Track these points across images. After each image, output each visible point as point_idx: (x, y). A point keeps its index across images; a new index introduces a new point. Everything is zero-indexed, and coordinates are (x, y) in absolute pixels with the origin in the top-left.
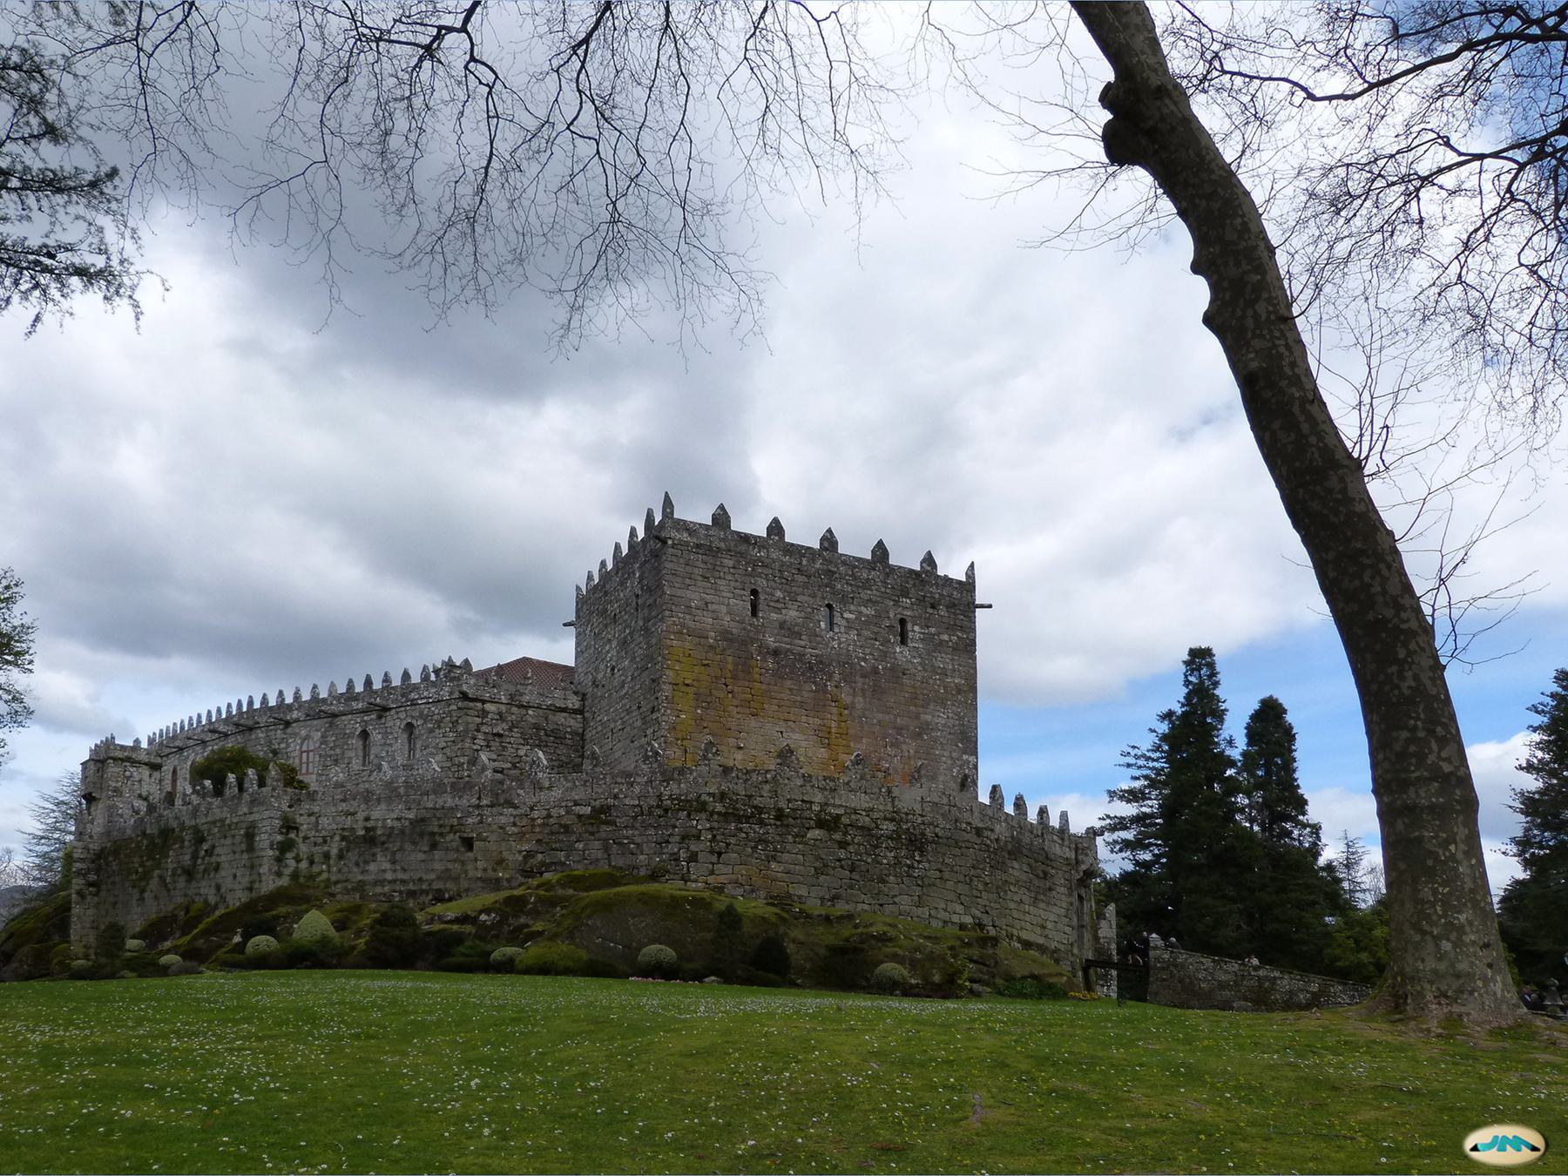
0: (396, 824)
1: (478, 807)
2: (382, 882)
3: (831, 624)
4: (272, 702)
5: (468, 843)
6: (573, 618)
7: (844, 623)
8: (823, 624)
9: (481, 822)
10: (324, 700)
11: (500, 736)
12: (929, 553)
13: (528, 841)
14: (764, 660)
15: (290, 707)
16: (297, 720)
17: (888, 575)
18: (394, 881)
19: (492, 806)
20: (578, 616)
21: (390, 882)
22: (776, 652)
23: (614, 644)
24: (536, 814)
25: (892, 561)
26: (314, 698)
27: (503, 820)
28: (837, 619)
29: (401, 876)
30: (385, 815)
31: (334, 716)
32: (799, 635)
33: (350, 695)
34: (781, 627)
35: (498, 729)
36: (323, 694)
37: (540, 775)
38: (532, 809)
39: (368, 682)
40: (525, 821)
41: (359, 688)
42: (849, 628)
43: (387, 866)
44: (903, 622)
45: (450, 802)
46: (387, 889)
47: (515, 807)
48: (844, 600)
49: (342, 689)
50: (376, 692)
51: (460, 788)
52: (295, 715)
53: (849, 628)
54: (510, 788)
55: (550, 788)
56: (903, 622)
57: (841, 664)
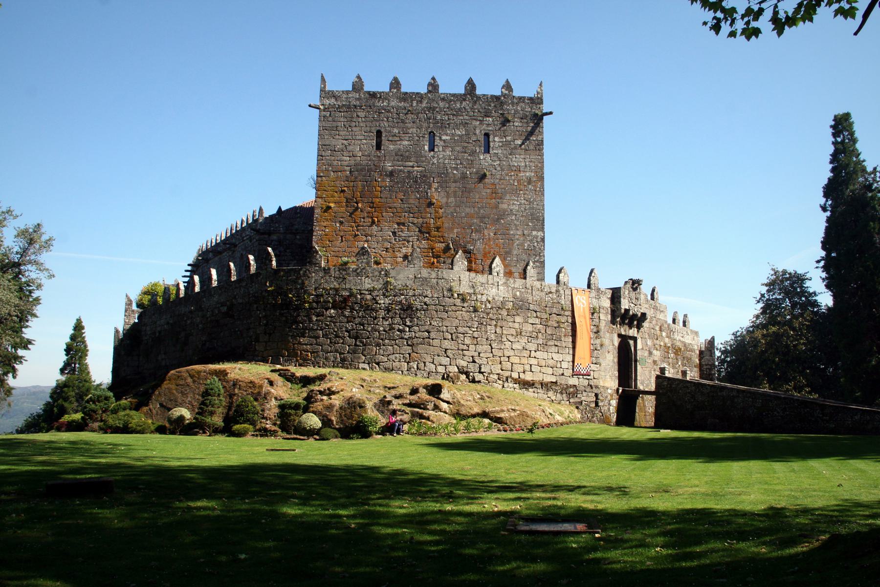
3: (432, 149)
7: (442, 143)
8: (426, 148)
12: (507, 81)
14: (383, 180)
17: (475, 102)
22: (391, 174)
25: (479, 92)
28: (437, 141)
32: (408, 159)
34: (396, 155)
42: (445, 147)
44: (487, 135)
48: (443, 126)
53: (445, 147)
56: (487, 135)
57: (439, 175)
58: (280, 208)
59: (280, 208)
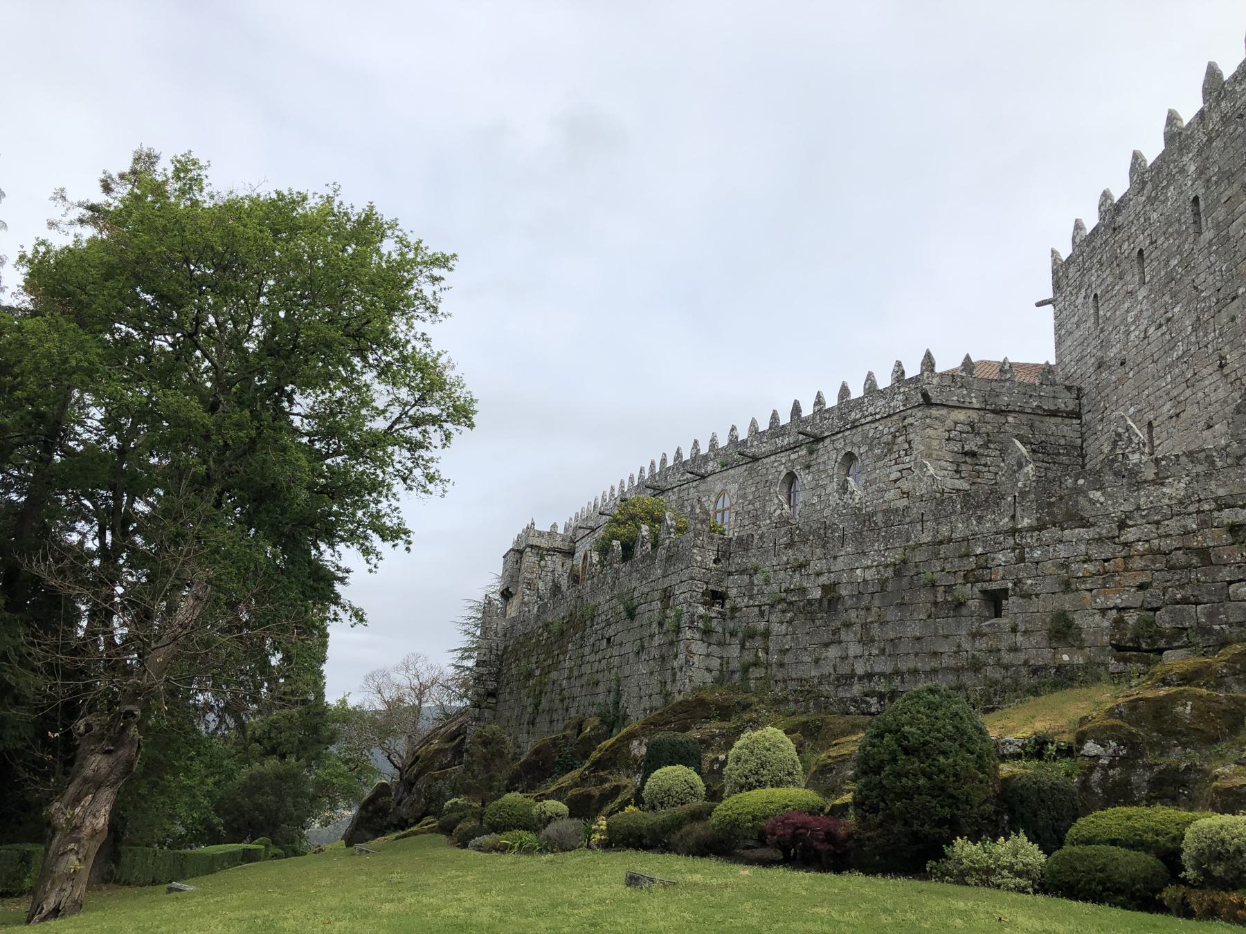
0: (869, 575)
1: (1014, 531)
2: (847, 679)
4: (686, 456)
5: (995, 601)
6: (1049, 295)
9: (1021, 559)
10: (744, 442)
11: (973, 454)
13: (1120, 588)
15: (705, 457)
16: (713, 473)
18: (869, 676)
19: (1041, 527)
20: (1057, 286)
21: (861, 678)
23: (1142, 294)
24: (1130, 535)
26: (733, 441)
27: (1062, 552)
29: (882, 666)
30: (859, 568)
31: (755, 459)
33: (776, 429)
35: (970, 446)
36: (743, 434)
37: (1134, 458)
38: (1122, 525)
39: (796, 409)
40: (1107, 550)
41: (785, 419)
43: (854, 649)
45: (961, 530)
46: (857, 689)
47: (1085, 523)
49: (764, 426)
50: (805, 421)
51: (973, 503)
52: (711, 466)
54: (1078, 491)
55: (1159, 481)
58: (968, 357)
59: (968, 357)
